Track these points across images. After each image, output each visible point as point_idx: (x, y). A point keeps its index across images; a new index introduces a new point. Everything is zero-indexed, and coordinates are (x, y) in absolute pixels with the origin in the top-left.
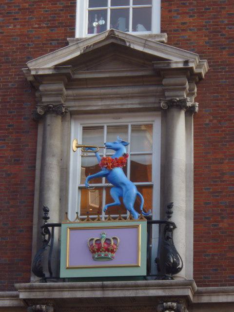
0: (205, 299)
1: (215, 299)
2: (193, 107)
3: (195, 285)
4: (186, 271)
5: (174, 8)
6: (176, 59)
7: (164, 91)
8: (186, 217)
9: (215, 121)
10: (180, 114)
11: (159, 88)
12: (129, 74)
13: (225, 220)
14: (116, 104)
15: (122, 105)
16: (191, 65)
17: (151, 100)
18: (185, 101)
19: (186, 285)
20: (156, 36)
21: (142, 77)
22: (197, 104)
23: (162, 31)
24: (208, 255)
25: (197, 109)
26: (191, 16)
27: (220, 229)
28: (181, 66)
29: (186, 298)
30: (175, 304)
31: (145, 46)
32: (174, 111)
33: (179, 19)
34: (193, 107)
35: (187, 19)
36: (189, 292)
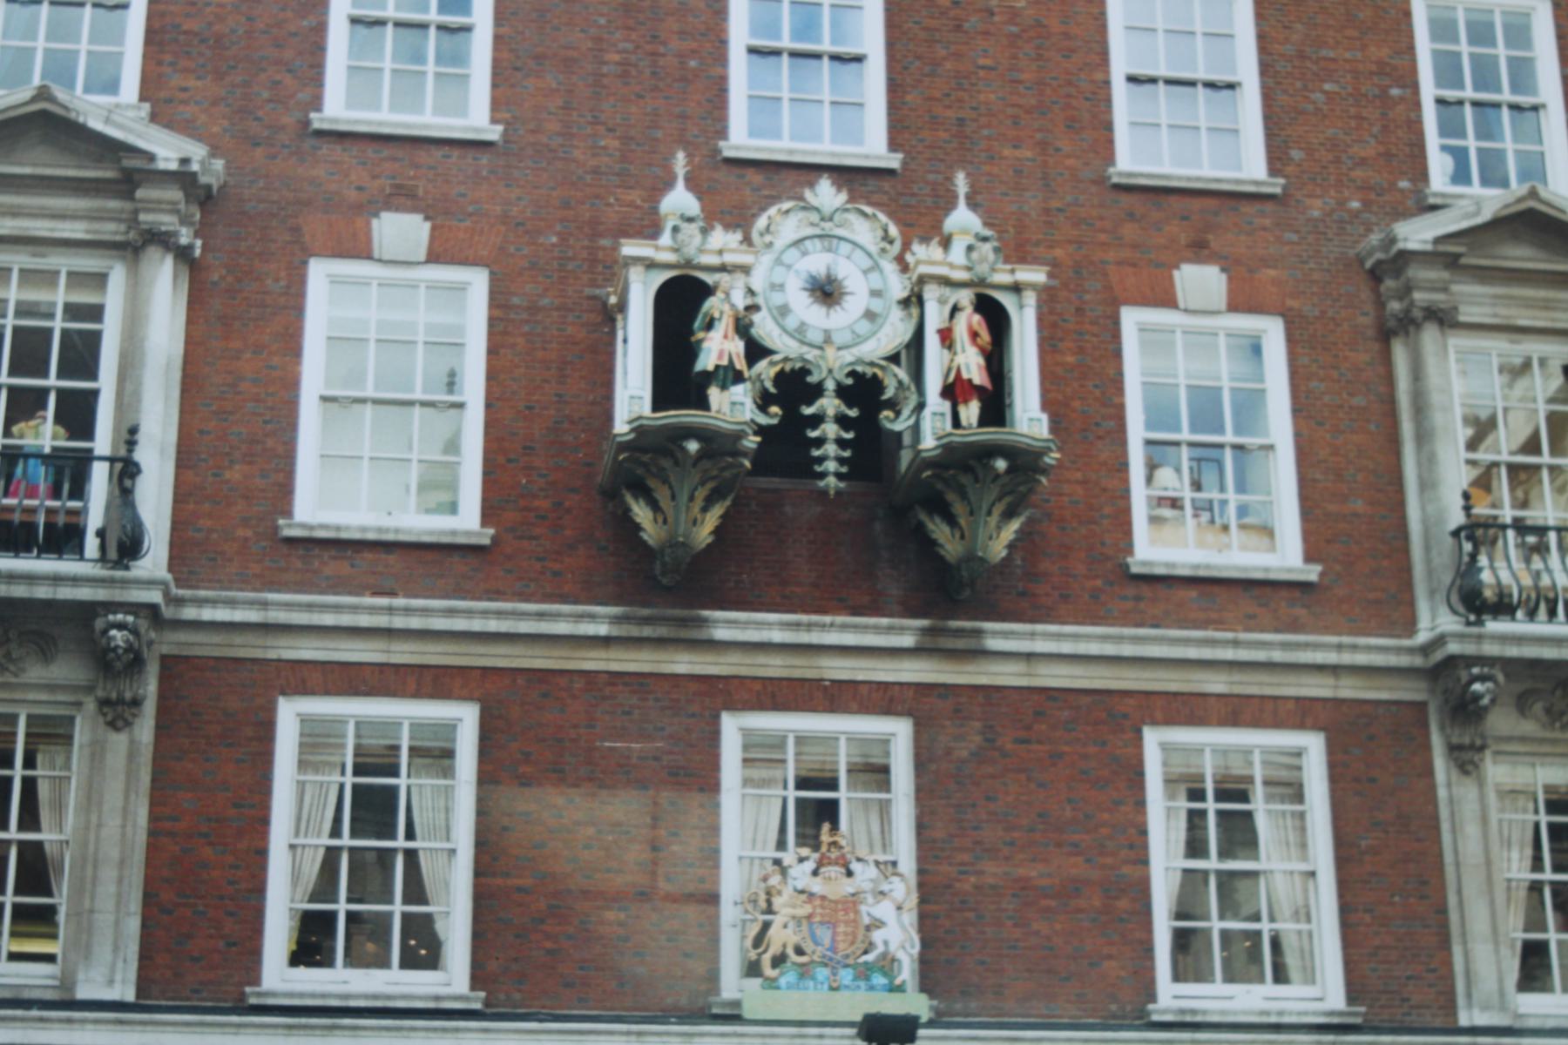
0: (189, 613)
1: (208, 614)
2: (190, 247)
3: (172, 585)
4: (154, 561)
5: (168, 58)
6: (168, 149)
7: (136, 212)
8: (162, 451)
9: (230, 279)
10: (163, 259)
11: (128, 205)
12: (71, 173)
13: (237, 467)
14: (41, 228)
15: (52, 230)
16: (195, 167)
17: (111, 226)
18: (175, 234)
19: (150, 583)
20: (128, 107)
21: (97, 180)
22: (199, 243)
23: (142, 98)
24: (199, 530)
25: (198, 252)
26: (199, 78)
27: (227, 482)
28: (173, 166)
29: (153, 609)
30: (130, 619)
31: (107, 121)
32: (153, 253)
33: (176, 80)
34: (190, 247)
35: (192, 83)
36: (155, 596)
